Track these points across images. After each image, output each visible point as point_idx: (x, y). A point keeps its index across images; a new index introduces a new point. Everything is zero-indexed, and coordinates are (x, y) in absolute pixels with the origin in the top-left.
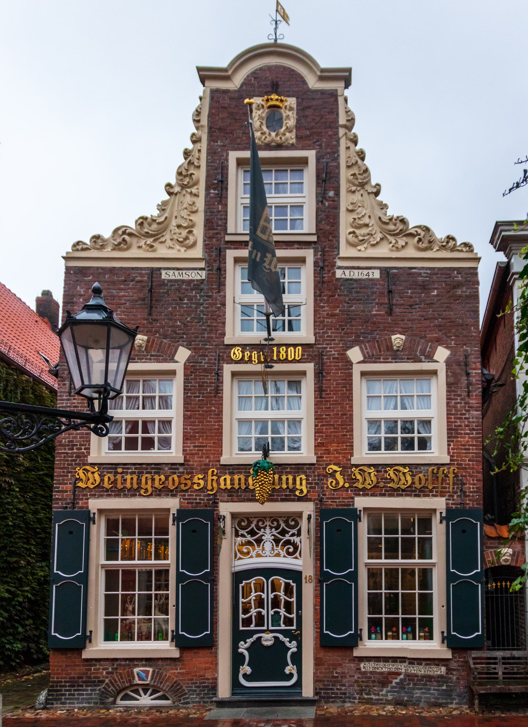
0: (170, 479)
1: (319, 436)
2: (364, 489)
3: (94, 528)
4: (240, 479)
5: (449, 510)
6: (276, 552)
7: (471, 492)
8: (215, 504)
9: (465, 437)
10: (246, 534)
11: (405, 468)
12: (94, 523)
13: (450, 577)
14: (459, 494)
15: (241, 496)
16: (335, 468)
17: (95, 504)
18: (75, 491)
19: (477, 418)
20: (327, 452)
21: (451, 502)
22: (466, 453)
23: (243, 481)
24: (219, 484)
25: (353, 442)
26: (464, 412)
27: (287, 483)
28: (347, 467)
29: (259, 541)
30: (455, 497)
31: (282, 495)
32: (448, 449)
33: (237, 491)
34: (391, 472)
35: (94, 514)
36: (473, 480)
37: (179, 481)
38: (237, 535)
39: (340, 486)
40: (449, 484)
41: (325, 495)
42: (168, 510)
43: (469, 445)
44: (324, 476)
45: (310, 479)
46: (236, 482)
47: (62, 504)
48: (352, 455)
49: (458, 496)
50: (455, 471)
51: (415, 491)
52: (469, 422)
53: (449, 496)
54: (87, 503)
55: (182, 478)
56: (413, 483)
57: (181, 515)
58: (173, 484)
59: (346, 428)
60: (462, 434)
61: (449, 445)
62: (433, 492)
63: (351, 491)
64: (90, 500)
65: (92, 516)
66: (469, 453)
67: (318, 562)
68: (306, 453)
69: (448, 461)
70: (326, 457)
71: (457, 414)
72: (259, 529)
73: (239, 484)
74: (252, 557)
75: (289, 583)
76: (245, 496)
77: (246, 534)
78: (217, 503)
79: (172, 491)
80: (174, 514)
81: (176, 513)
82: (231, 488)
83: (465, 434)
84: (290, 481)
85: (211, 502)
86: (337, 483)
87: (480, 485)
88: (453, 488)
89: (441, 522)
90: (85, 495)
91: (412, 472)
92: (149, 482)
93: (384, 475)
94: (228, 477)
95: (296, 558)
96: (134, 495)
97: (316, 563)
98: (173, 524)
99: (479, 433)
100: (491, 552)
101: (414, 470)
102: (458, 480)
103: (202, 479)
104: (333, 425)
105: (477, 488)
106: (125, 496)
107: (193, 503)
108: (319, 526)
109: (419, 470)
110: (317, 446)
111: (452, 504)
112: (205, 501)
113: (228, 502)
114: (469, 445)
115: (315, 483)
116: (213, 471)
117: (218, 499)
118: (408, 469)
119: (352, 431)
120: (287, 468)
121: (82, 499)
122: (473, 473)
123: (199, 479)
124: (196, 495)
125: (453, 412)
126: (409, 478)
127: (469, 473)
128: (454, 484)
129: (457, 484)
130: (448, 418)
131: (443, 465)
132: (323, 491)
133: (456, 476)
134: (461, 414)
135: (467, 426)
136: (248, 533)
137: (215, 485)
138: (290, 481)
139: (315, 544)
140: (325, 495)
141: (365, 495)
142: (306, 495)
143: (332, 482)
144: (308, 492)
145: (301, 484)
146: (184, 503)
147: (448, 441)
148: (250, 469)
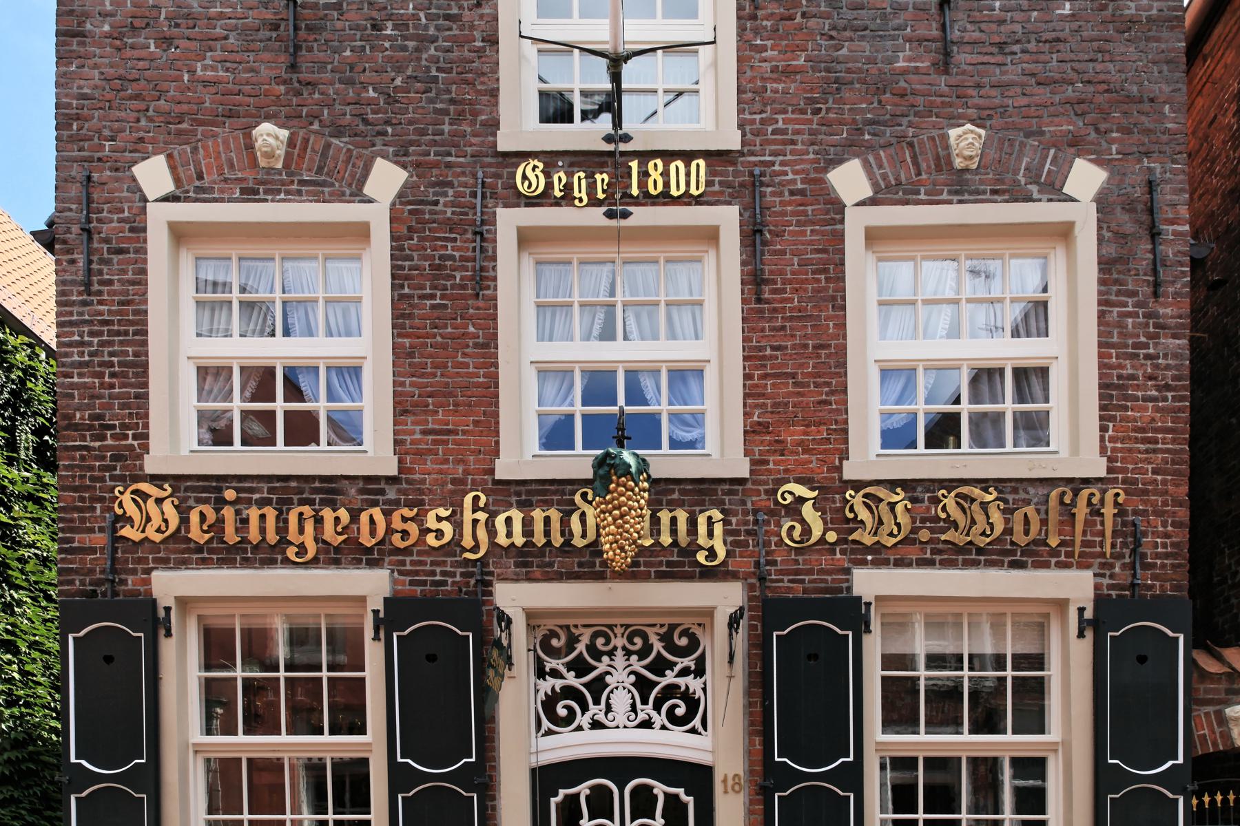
0: (364, 517)
1: (756, 406)
2: (878, 548)
3: (168, 648)
4: (547, 521)
5: (1100, 600)
6: (642, 716)
7: (1157, 556)
8: (485, 585)
9: (1146, 409)
10: (563, 670)
11: (986, 490)
12: (169, 634)
13: (1104, 779)
14: (1127, 560)
15: (551, 564)
16: (801, 490)
17: (168, 585)
18: (115, 550)
19: (1176, 356)
20: (778, 447)
21: (1106, 581)
22: (1147, 451)
23: (556, 526)
24: (492, 532)
25: (846, 422)
26: (1143, 339)
27: (674, 532)
28: (832, 491)
29: (598, 687)
30: (1117, 570)
31: (661, 563)
32: (1102, 439)
33: (541, 552)
34: (950, 502)
35: (168, 609)
36: (1164, 525)
37: (388, 523)
38: (541, 673)
39: (813, 540)
40: (1102, 534)
41: (774, 563)
42: (362, 600)
43: (1156, 430)
44: (771, 513)
45: (734, 520)
46: (539, 527)
47: (82, 583)
48: (844, 455)
49: (1124, 566)
50: (1120, 500)
51: (1013, 553)
52: (1157, 367)
53: (1102, 565)
54: (147, 582)
55: (396, 517)
56: (1008, 531)
57: (395, 613)
58: (373, 533)
59: (828, 384)
60: (1136, 399)
61: (1103, 429)
62: (1058, 554)
63: (843, 552)
64: (154, 574)
65: (162, 614)
66: (1155, 451)
67: (757, 740)
68: (722, 452)
69: (1102, 473)
70: (775, 463)
71: (1126, 346)
72: (597, 655)
73: (547, 533)
74: (579, 728)
75: (677, 796)
76: (562, 564)
77: (563, 670)
78: (490, 584)
79: (369, 550)
80: (376, 612)
81: (381, 607)
82: (525, 545)
83: (1145, 399)
84: (682, 526)
85: (473, 582)
86: (807, 531)
87: (1183, 536)
88: (1113, 546)
89: (1081, 635)
90: (140, 560)
91: (1006, 501)
92: (309, 527)
93: (928, 509)
94: (517, 516)
95: (693, 731)
96: (269, 562)
97: (751, 743)
98: (376, 638)
99: (1182, 399)
100: (1207, 714)
101: (1010, 497)
102: (1124, 524)
103: (447, 519)
104: (793, 376)
105: (1173, 544)
106: (247, 563)
107: (424, 583)
108: (759, 646)
109: (1022, 495)
110: (751, 432)
111: (1110, 587)
112: (458, 578)
113: (517, 580)
114: (1156, 430)
115: (748, 533)
116: (476, 498)
117: (491, 573)
118: (995, 494)
119: (845, 391)
120: (673, 491)
121: (134, 571)
122: (1165, 503)
123: (439, 519)
124: (432, 563)
125: (1115, 339)
126: (996, 517)
127: (1154, 504)
128: (1115, 533)
129: (1125, 535)
130: (1101, 356)
131: (1086, 481)
132: (768, 553)
133: (1121, 512)
134: (1135, 346)
135: (1151, 378)
136: (570, 667)
137: (482, 534)
138: (682, 526)
139: (748, 693)
140: (774, 563)
141: (878, 563)
142: (724, 563)
143: (792, 528)
144: (729, 554)
145: (710, 534)
146: (403, 583)
147: (1101, 418)
148: (573, 493)
